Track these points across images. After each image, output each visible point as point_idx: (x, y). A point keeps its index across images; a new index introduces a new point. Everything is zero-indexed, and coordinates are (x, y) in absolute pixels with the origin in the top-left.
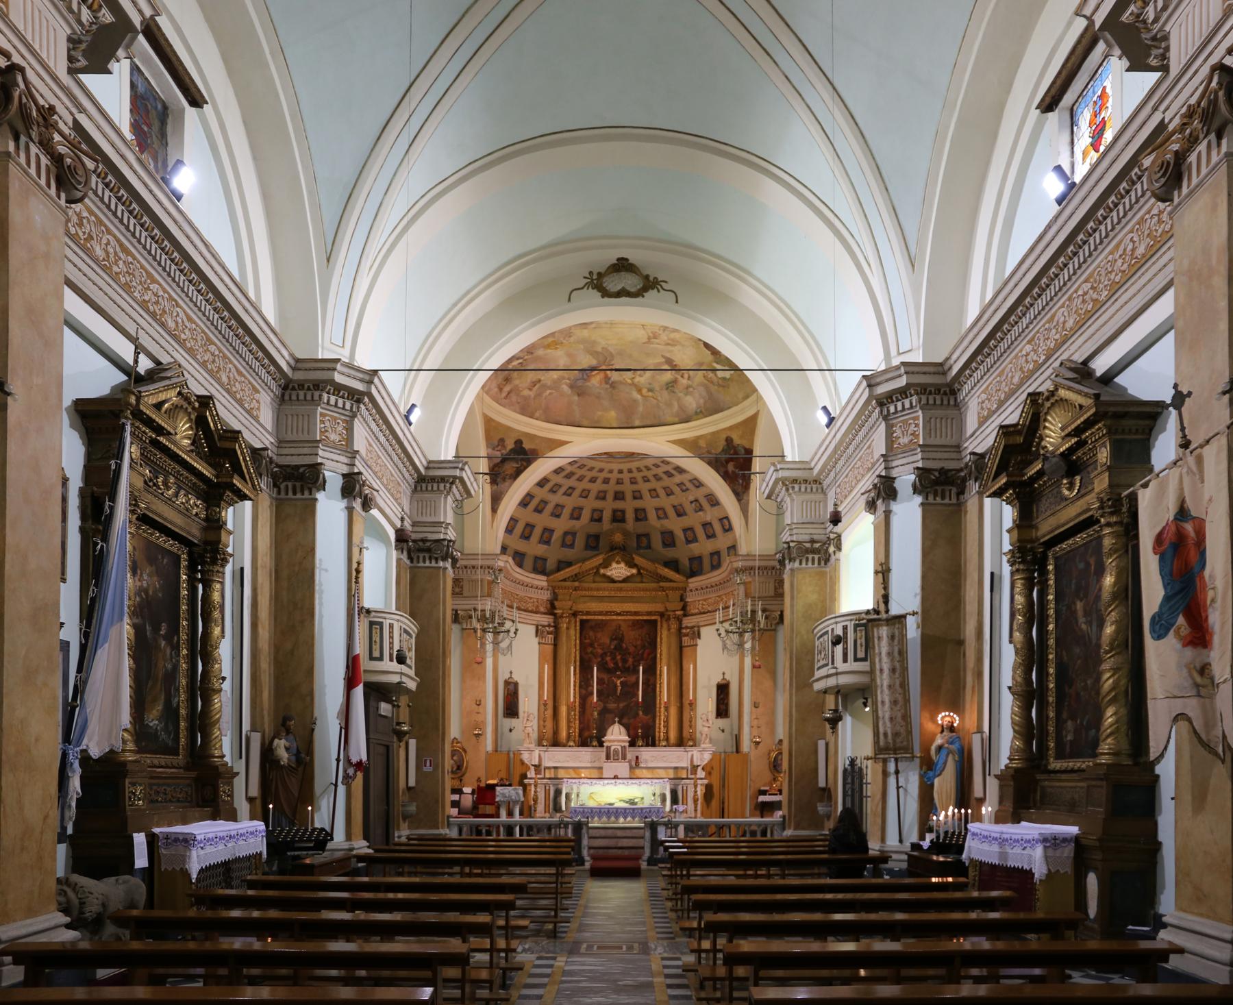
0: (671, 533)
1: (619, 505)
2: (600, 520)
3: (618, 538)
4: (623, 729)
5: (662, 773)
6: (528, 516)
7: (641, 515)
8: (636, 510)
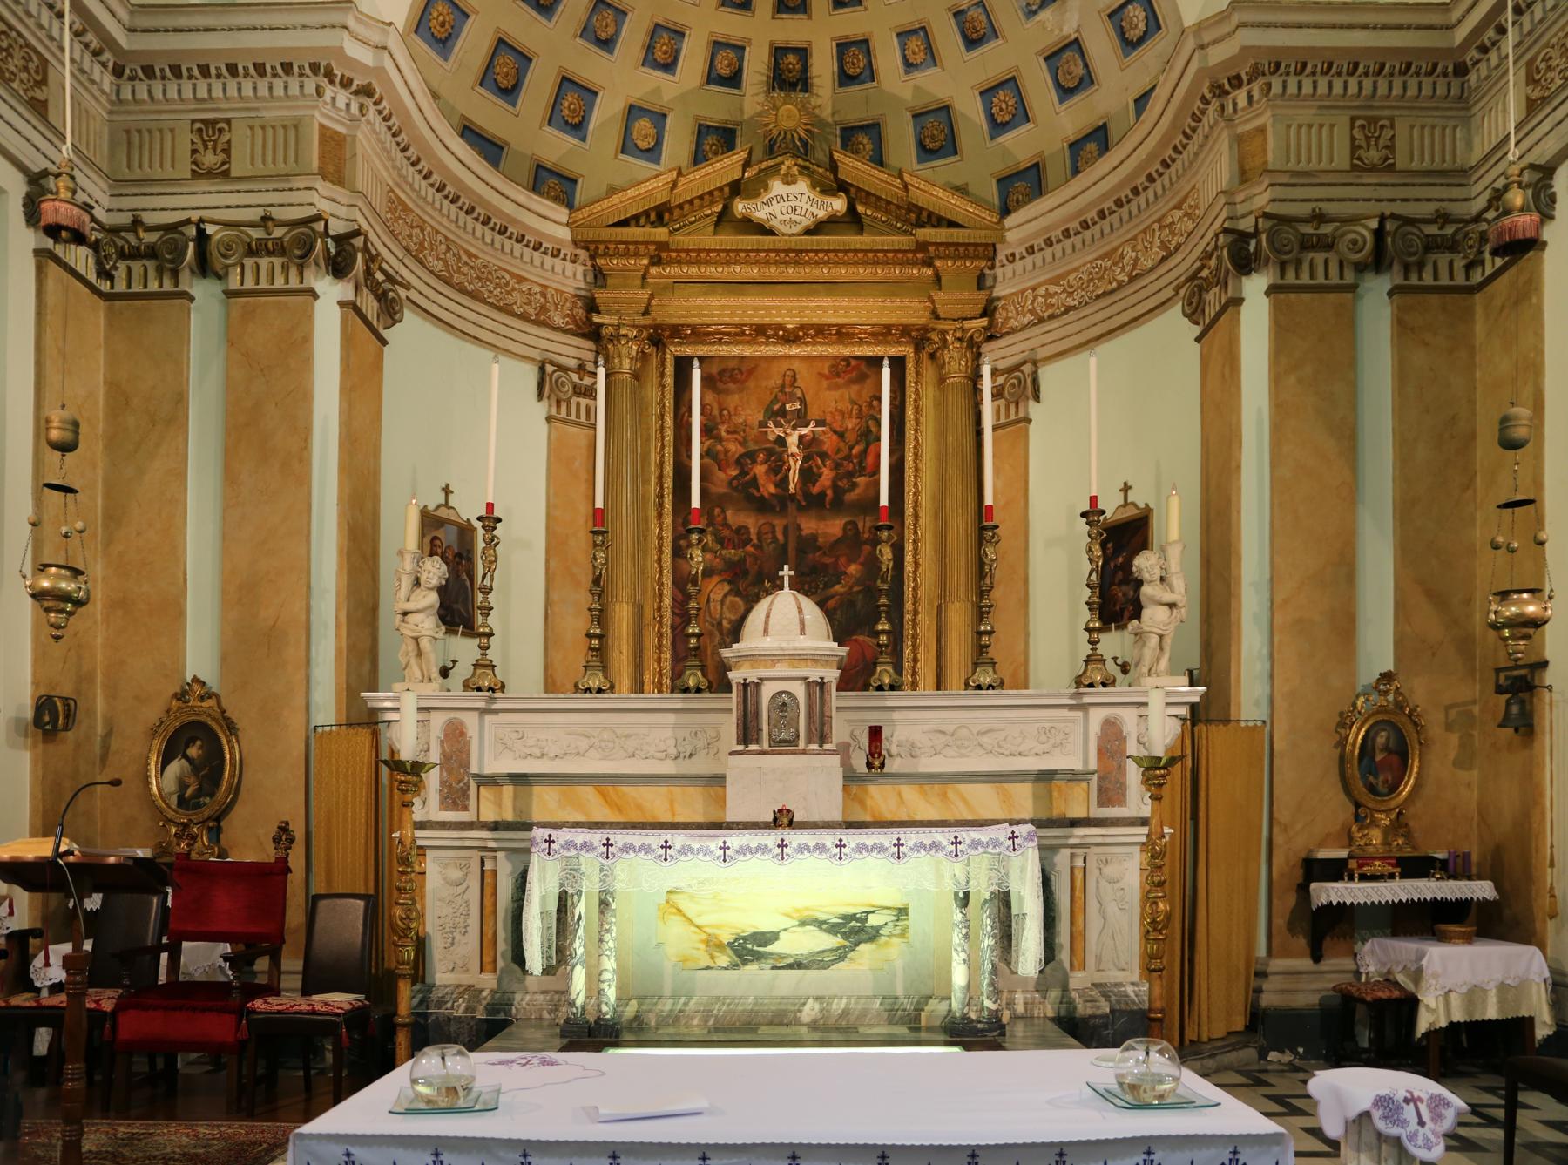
2: (733, 80)
4: (810, 607)
5: (984, 800)
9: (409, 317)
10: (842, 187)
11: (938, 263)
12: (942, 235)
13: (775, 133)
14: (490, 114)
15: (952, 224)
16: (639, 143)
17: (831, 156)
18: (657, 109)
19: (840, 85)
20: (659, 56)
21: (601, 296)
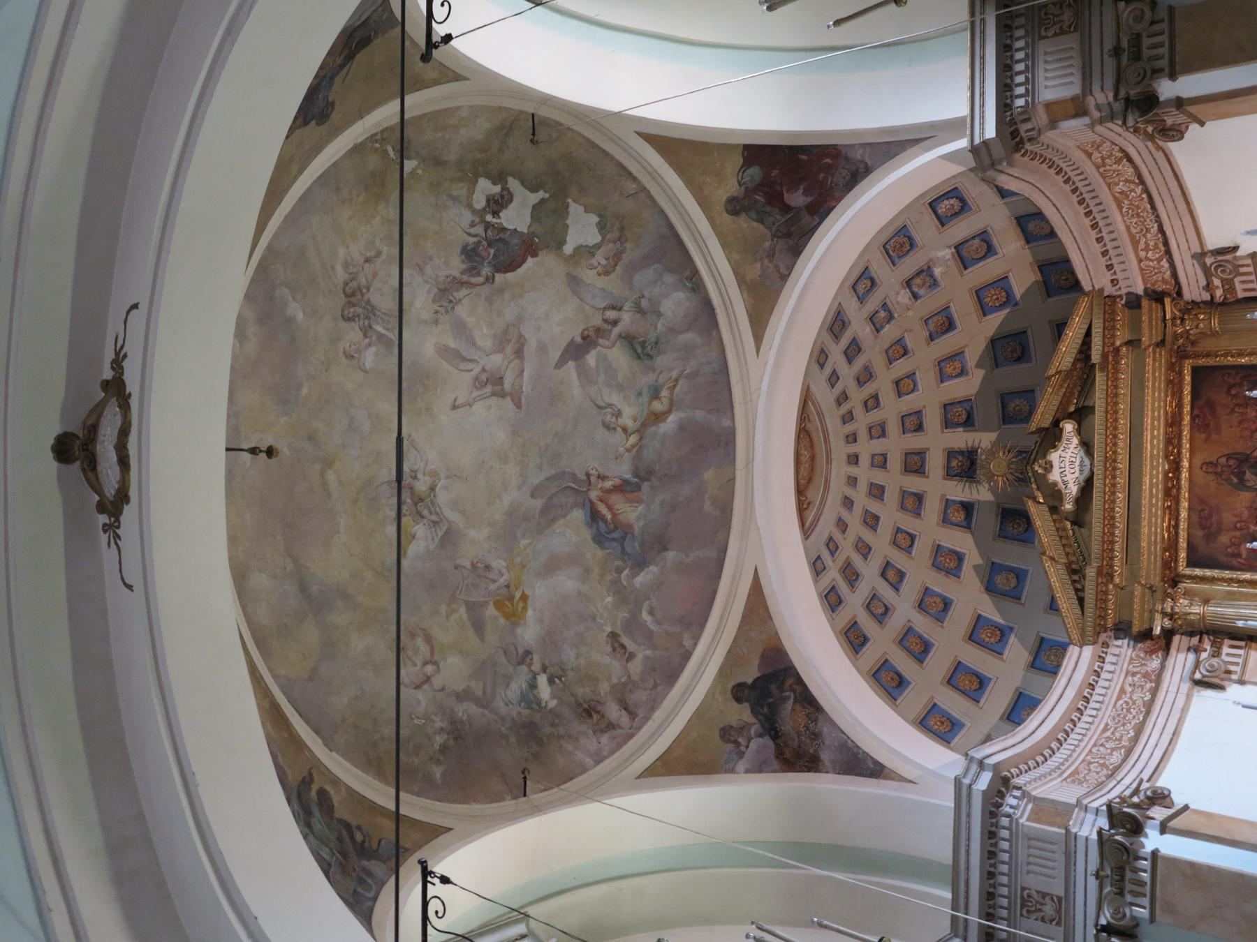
0: (994, 342)
1: (935, 463)
2: (968, 508)
3: (999, 465)
6: (927, 682)
7: (960, 415)
8: (948, 424)
9: (1162, 782)
10: (1056, 423)
11: (1118, 343)
12: (1097, 341)
13: (1010, 477)
14: (998, 699)
15: (1088, 333)
16: (1013, 585)
17: (1032, 433)
18: (988, 569)
19: (973, 425)
20: (953, 565)
21: (1135, 629)
